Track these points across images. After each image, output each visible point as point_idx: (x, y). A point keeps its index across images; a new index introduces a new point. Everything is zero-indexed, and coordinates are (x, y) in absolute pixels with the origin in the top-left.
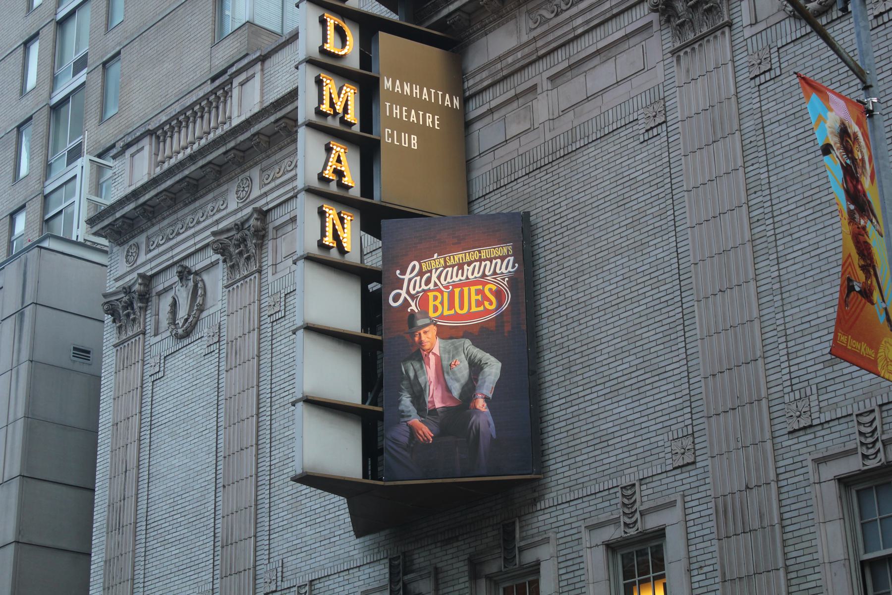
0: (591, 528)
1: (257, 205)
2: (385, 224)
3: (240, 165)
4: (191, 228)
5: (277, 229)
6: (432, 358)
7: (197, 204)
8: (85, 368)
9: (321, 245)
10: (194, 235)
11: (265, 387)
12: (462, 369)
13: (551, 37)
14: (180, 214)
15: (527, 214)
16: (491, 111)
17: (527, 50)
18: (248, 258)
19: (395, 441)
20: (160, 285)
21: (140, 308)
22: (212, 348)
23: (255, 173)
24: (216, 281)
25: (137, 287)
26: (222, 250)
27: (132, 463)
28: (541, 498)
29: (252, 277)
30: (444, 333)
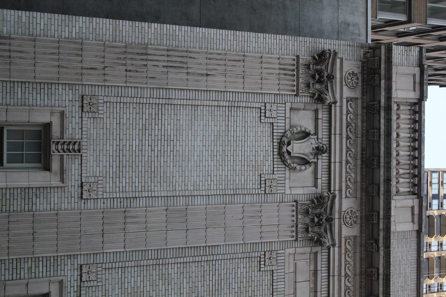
4: (347, 152)
5: (316, 254)
7: (359, 162)
14: (359, 140)
18: (307, 230)
20: (323, 115)
21: (314, 94)
22: (263, 186)
29: (294, 234)
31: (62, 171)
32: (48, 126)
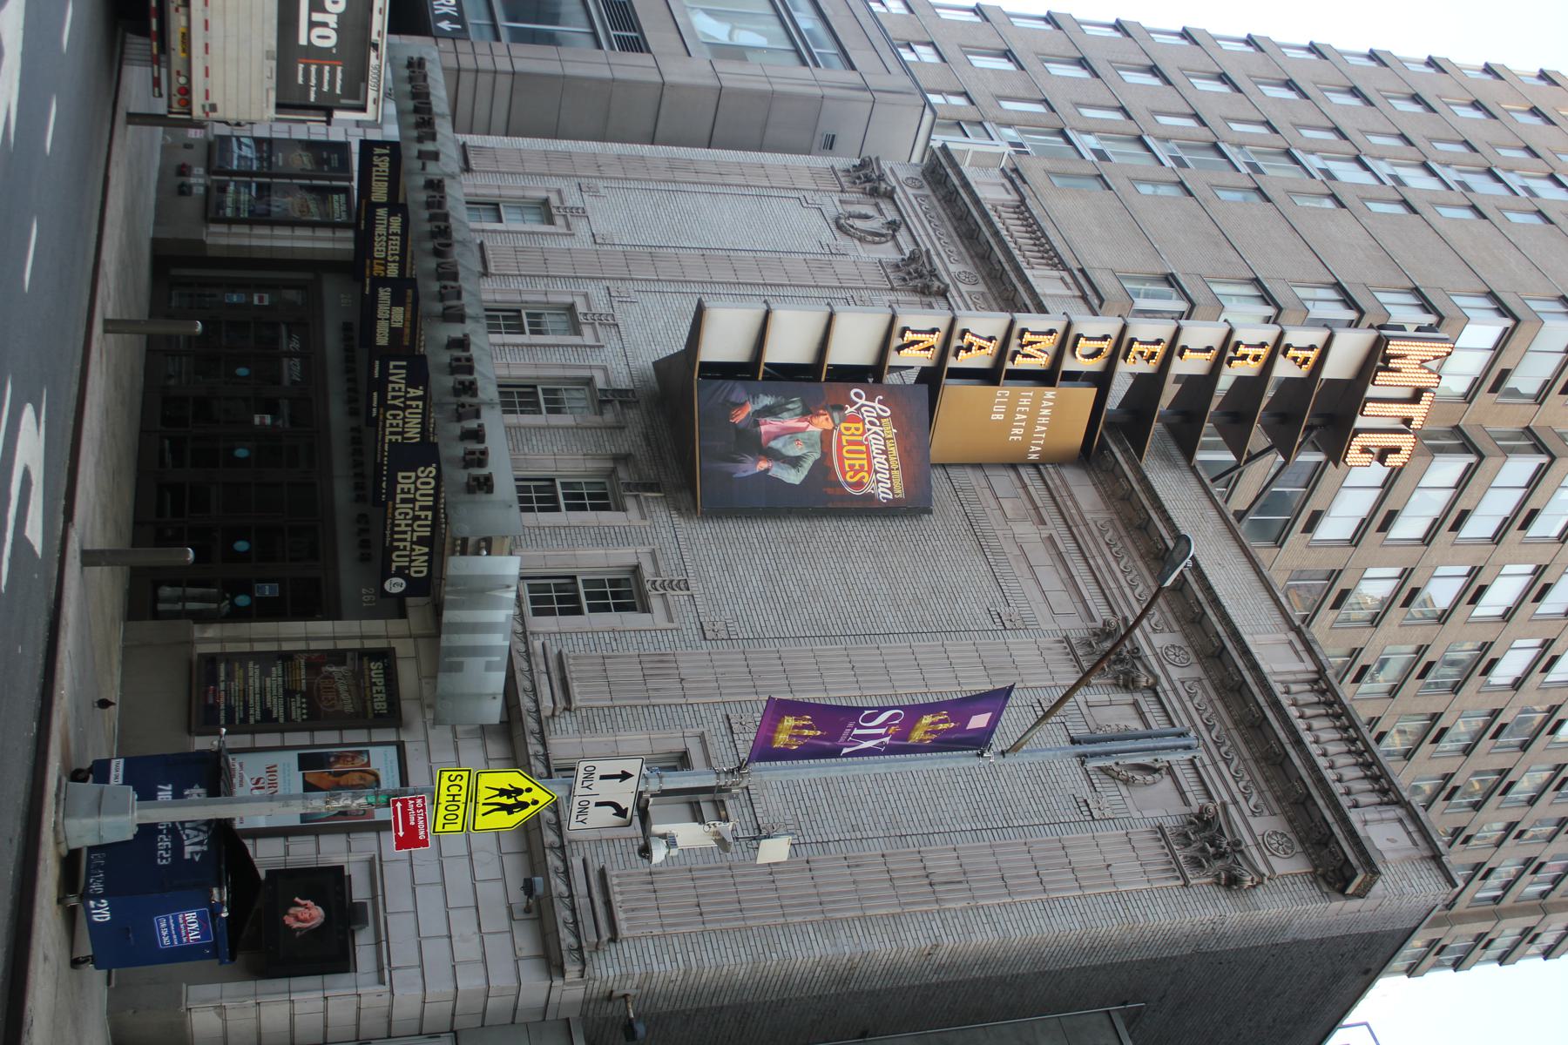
0: (653, 553)
1: (952, 288)
2: (925, 388)
3: (989, 275)
6: (804, 424)
7: (956, 239)
8: (816, 145)
9: (905, 330)
10: (928, 235)
11: (789, 291)
12: (794, 450)
13: (1087, 538)
14: (948, 224)
15: (930, 512)
16: (1025, 487)
17: (1077, 518)
19: (732, 390)
20: (886, 206)
23: (981, 288)
24: (887, 252)
25: (883, 185)
26: (913, 258)
27: (728, 180)
28: (681, 514)
30: (826, 436)
31: (568, 226)
32: (546, 202)
